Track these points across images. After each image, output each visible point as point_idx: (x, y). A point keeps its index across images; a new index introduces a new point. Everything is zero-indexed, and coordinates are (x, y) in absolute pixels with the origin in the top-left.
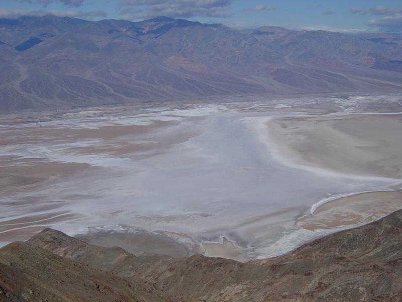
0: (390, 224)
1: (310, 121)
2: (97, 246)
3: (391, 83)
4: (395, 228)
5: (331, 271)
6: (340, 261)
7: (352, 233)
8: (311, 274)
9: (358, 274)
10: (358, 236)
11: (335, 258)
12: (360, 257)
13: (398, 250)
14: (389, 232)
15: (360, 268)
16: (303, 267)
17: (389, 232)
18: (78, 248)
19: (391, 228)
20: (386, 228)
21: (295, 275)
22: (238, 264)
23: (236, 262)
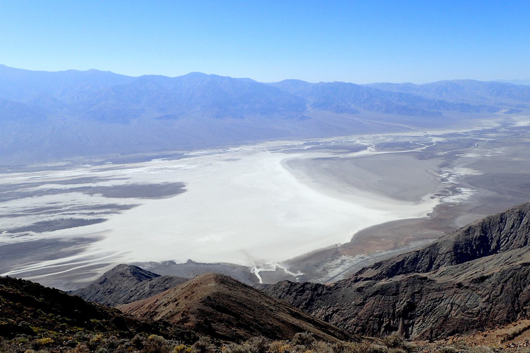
1: (335, 160)
2: (183, 278)
4: (452, 250)
5: (416, 290)
6: (423, 281)
8: (399, 294)
9: (443, 292)
11: (418, 279)
15: (445, 287)
16: (389, 288)
18: (165, 281)
21: (382, 296)
22: (326, 287)
23: (324, 285)
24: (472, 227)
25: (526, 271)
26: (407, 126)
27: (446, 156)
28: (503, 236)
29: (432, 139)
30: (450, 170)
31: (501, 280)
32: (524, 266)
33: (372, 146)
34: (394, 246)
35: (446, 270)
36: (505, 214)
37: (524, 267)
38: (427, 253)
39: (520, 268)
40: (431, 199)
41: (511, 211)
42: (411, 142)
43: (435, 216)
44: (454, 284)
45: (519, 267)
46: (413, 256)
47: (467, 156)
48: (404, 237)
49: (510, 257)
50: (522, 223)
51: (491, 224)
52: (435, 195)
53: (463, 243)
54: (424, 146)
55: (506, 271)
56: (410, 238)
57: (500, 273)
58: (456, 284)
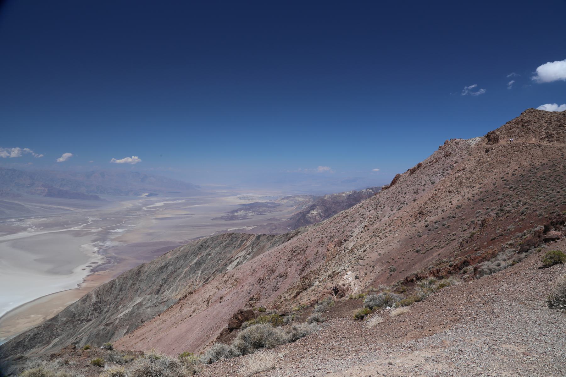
0: (65, 318)
3: (62, 207)
4: (70, 319)
7: (32, 332)
10: (38, 333)
12: (41, 350)
13: (72, 336)
14: (65, 324)
17: (65, 324)
19: (65, 320)
20: (62, 321)
24: (89, 296)
25: (108, 330)
26: (68, 208)
27: (98, 233)
28: (113, 299)
29: (88, 218)
30: (101, 244)
31: (88, 342)
32: (107, 326)
33: (32, 227)
34: (43, 320)
35: (59, 339)
36: (116, 280)
37: (106, 327)
38: (48, 327)
39: (103, 329)
40: (82, 271)
41: (120, 277)
42: (69, 222)
43: (84, 285)
44: (48, 356)
45: (103, 327)
46: (36, 331)
47: (116, 231)
48: (54, 309)
49: (105, 319)
50: (128, 286)
51: (105, 290)
52: (87, 266)
53: (81, 311)
54: (81, 225)
55: (93, 333)
56: (60, 309)
57: (88, 336)
58: (50, 356)
